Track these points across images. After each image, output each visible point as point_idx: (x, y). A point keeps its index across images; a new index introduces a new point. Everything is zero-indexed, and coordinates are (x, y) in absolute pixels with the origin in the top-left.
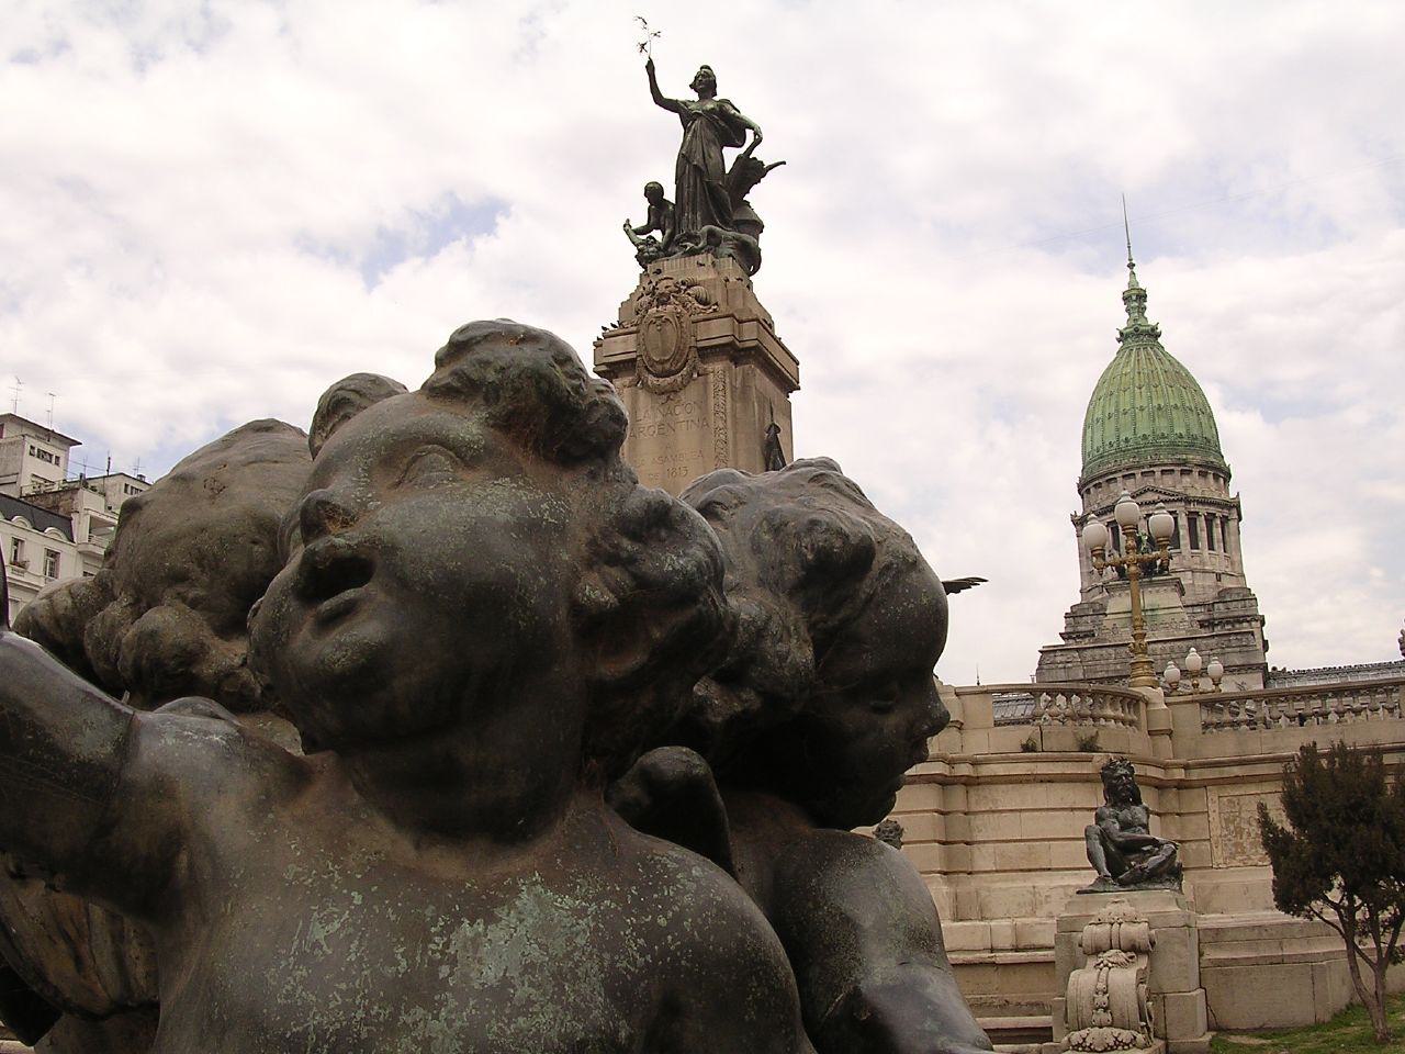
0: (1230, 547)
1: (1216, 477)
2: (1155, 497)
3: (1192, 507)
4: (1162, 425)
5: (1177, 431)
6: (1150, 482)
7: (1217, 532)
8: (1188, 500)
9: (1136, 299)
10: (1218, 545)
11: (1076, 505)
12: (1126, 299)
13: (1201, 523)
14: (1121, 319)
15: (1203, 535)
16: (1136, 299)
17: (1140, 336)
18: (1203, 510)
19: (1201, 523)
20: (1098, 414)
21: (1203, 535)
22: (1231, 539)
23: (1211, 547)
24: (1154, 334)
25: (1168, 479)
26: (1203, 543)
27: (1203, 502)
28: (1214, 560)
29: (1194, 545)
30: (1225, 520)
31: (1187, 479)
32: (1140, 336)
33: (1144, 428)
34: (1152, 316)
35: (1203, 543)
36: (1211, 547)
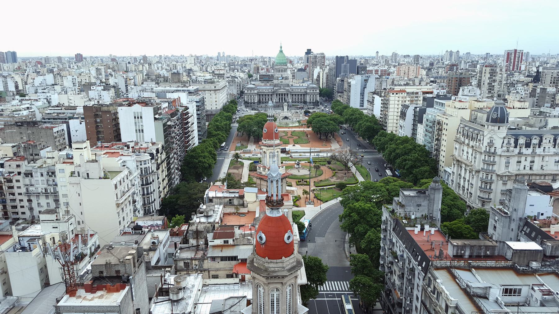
9: (281, 47)
14: (279, 49)
16: (281, 47)
17: (281, 51)
34: (282, 49)
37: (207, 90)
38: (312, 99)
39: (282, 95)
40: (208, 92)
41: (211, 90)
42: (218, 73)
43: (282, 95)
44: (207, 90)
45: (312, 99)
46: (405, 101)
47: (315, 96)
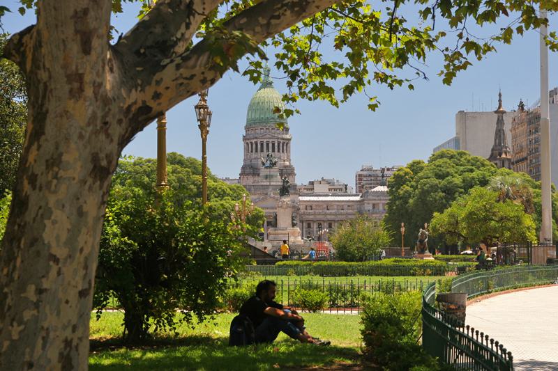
0: (288, 151)
7: (285, 147)
8: (278, 138)
10: (285, 151)
13: (281, 145)
15: (281, 148)
18: (282, 141)
19: (281, 145)
21: (281, 148)
22: (288, 149)
25: (273, 131)
26: (281, 151)
27: (283, 139)
28: (284, 156)
29: (279, 151)
30: (287, 143)
35: (281, 151)
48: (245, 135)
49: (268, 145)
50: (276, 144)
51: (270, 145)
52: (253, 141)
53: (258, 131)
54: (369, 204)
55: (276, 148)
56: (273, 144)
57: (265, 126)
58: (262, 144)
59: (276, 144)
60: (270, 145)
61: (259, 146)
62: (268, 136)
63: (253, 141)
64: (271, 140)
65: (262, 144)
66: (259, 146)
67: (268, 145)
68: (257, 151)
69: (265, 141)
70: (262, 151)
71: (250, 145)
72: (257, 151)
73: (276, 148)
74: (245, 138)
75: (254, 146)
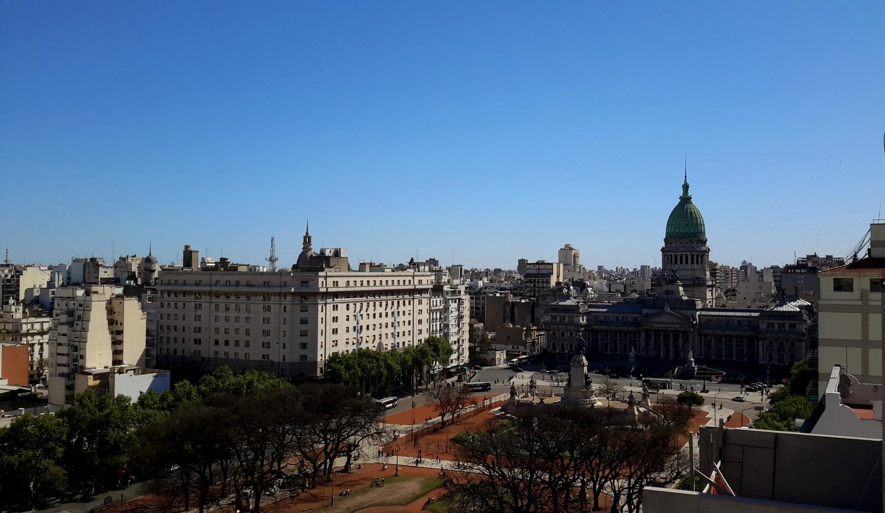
1: (702, 243)
2: (683, 250)
3: (693, 253)
4: (687, 229)
5: (691, 231)
6: (682, 244)
9: (686, 187)
10: (700, 263)
11: (663, 245)
12: (683, 186)
13: (695, 257)
14: (681, 193)
16: (686, 187)
17: (686, 200)
18: (696, 254)
19: (695, 257)
20: (670, 223)
23: (697, 263)
24: (690, 198)
25: (687, 245)
30: (702, 256)
31: (692, 245)
32: (686, 200)
33: (682, 231)
34: (690, 193)
36: (697, 263)
37: (275, 294)
38: (775, 356)
39: (676, 337)
40: (277, 298)
41: (285, 295)
42: (534, 272)
43: (667, 336)
44: (275, 294)
45: (775, 356)
46: (543, 282)
47: (787, 345)
48: (664, 247)
49: (681, 257)
50: (690, 257)
51: (684, 258)
52: (669, 254)
53: (673, 245)
54: (763, 323)
55: (690, 261)
56: (687, 257)
57: (679, 240)
58: (676, 257)
59: (690, 257)
60: (684, 258)
61: (673, 259)
62: (681, 249)
63: (669, 254)
64: (684, 253)
65: (676, 257)
66: (673, 259)
67: (681, 257)
68: (671, 263)
69: (679, 254)
70: (676, 263)
71: (666, 257)
72: (671, 263)
73: (690, 261)
74: (662, 250)
75: (670, 257)
